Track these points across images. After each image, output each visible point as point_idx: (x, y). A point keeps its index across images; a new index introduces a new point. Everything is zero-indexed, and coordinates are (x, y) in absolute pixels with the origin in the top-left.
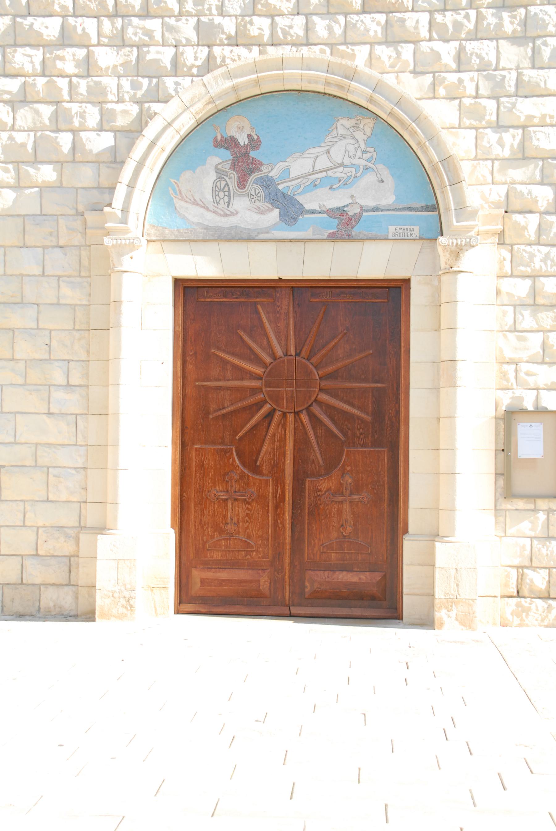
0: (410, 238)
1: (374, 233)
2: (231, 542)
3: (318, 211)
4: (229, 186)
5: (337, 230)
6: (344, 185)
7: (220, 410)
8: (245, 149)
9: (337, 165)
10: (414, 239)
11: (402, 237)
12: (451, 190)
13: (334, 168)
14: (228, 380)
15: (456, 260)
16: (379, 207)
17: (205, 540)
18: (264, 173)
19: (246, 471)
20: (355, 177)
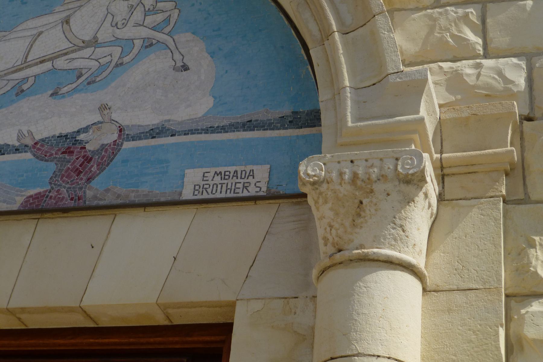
0: (241, 195)
1: (144, 189)
3: (13, 146)
5: (49, 188)
6: (89, 83)
9: (82, 45)
10: (254, 199)
11: (218, 195)
12: (345, 45)
13: (73, 52)
15: (354, 225)
16: (167, 125)
20: (117, 66)
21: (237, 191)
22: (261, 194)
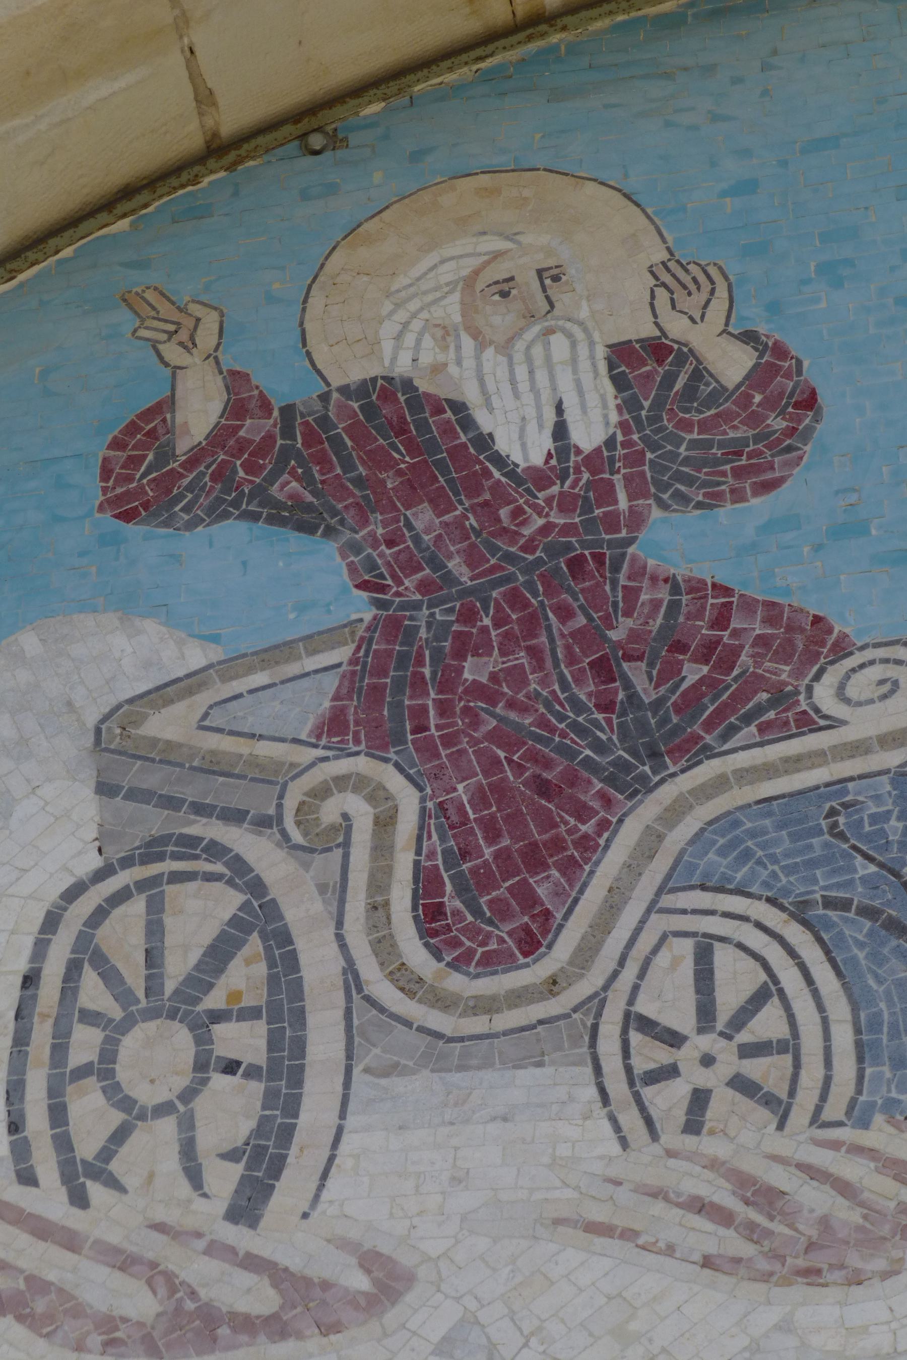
4: (284, 938)
8: (566, 503)
18: (858, 749)
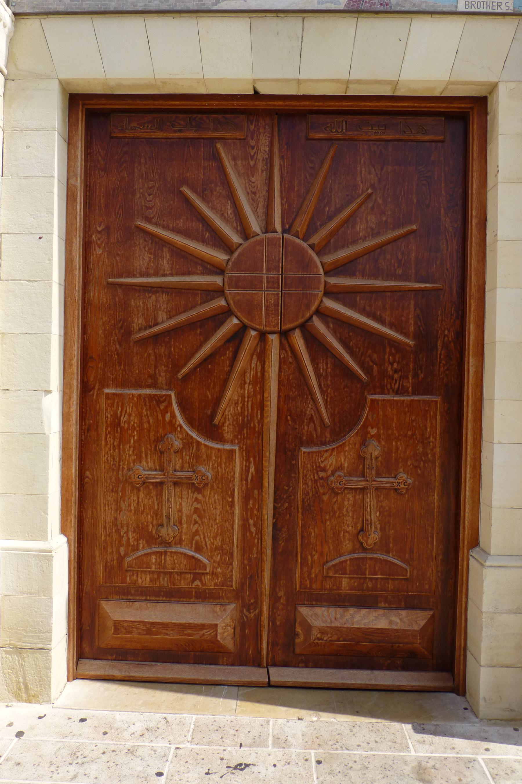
0: (496, 11)
2: (168, 559)
7: (150, 327)
11: (482, 10)
14: (164, 275)
17: (122, 553)
19: (194, 435)
21: (494, 8)
22: (510, 11)
